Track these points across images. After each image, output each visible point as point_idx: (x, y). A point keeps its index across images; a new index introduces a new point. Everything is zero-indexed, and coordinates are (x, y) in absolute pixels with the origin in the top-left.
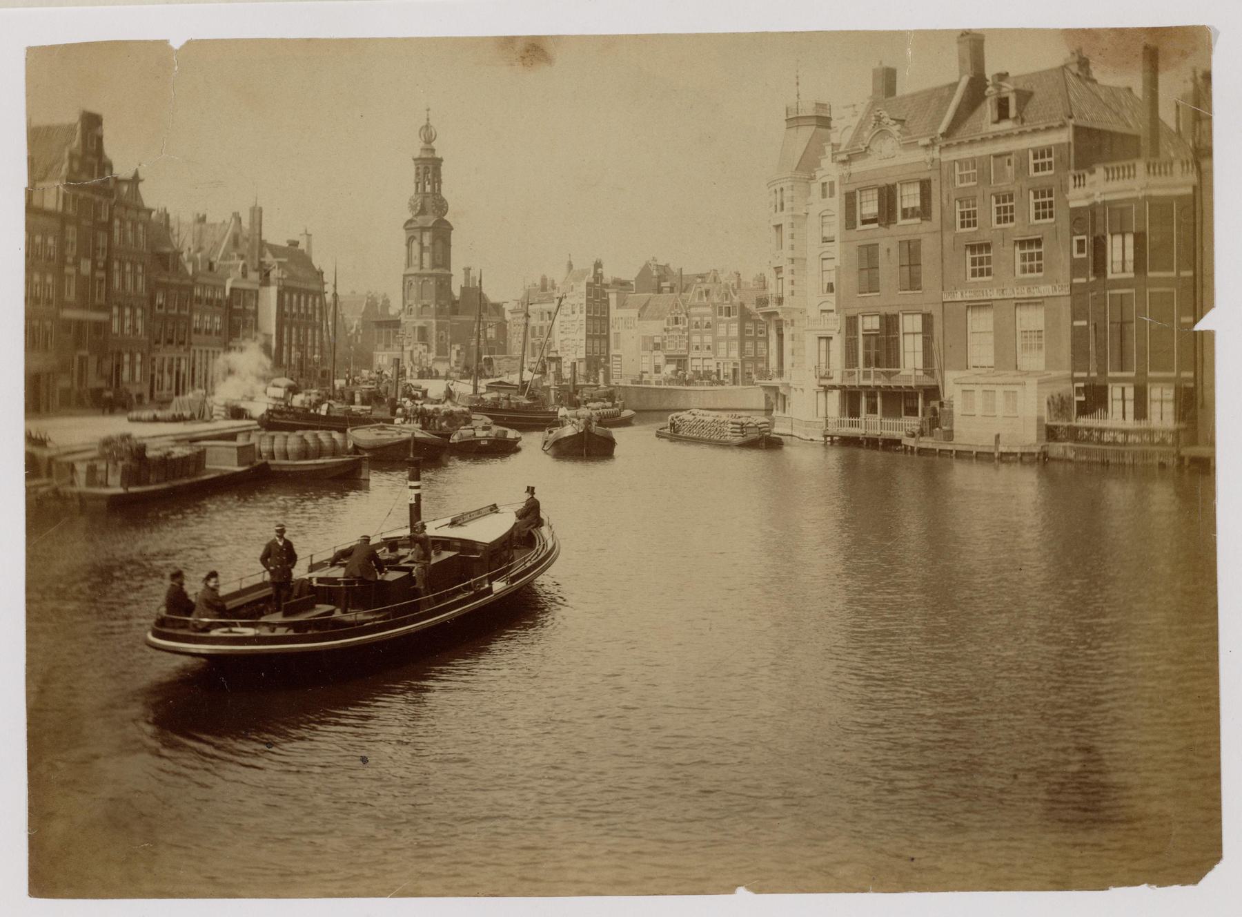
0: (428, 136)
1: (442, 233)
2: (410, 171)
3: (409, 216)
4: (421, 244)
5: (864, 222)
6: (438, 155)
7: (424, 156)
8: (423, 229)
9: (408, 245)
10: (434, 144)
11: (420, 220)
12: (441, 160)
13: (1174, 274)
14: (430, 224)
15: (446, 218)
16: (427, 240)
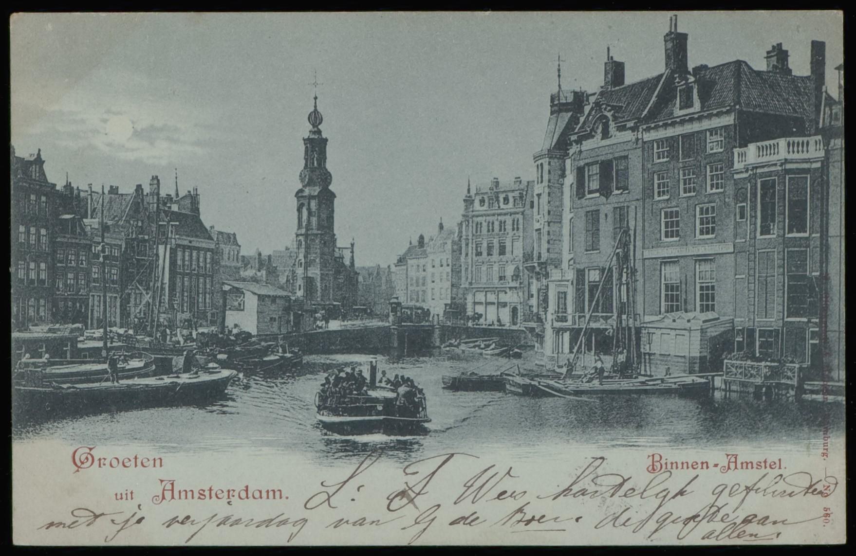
0: (315, 118)
1: (327, 198)
2: (301, 149)
3: (300, 186)
4: (309, 209)
5: (590, 192)
6: (324, 136)
7: (312, 136)
8: (311, 197)
9: (299, 210)
10: (320, 127)
11: (307, 192)
12: (326, 140)
13: (806, 235)
14: (316, 194)
15: (331, 188)
16: (313, 204)
